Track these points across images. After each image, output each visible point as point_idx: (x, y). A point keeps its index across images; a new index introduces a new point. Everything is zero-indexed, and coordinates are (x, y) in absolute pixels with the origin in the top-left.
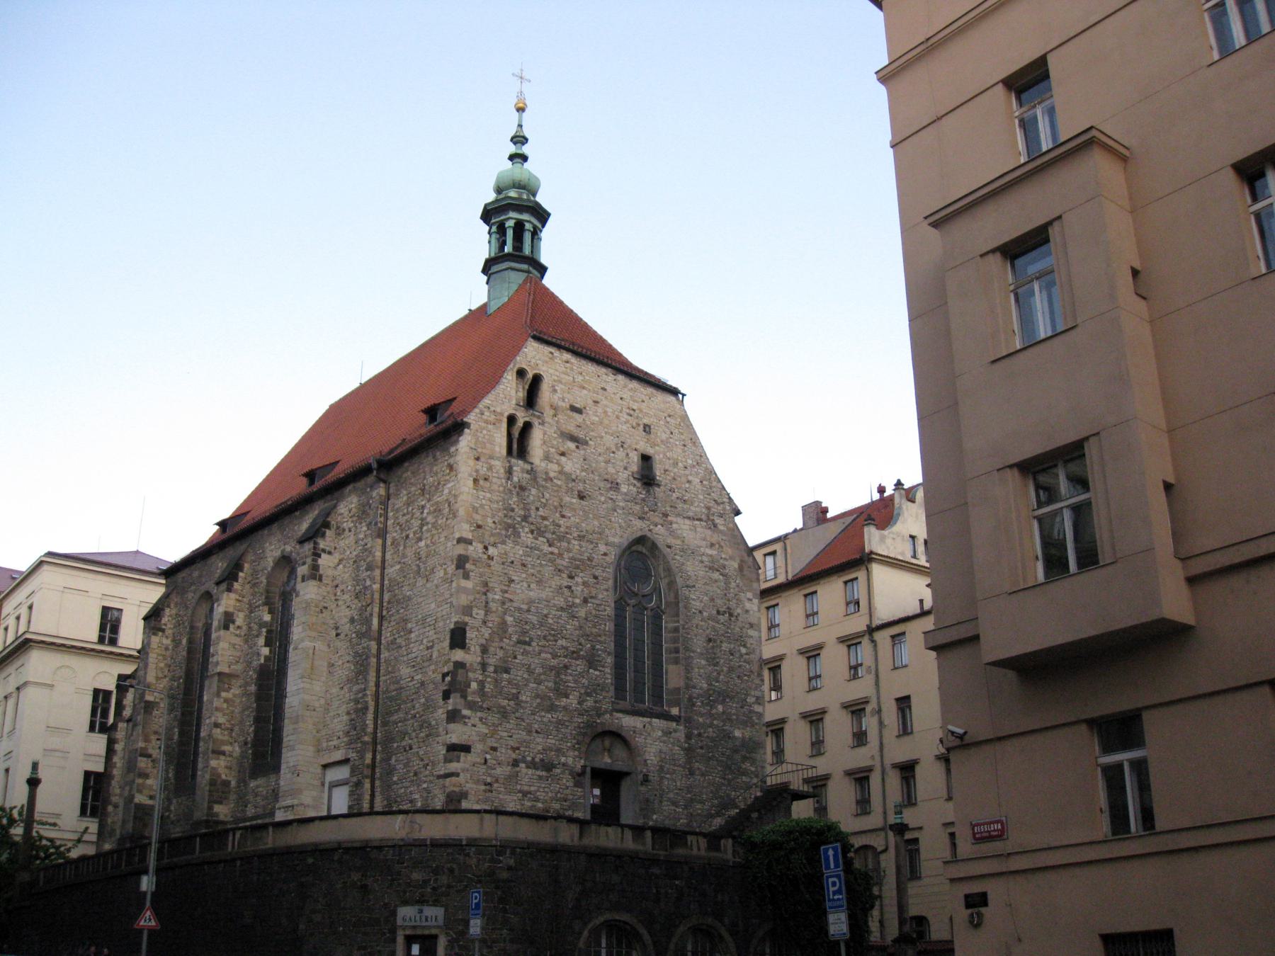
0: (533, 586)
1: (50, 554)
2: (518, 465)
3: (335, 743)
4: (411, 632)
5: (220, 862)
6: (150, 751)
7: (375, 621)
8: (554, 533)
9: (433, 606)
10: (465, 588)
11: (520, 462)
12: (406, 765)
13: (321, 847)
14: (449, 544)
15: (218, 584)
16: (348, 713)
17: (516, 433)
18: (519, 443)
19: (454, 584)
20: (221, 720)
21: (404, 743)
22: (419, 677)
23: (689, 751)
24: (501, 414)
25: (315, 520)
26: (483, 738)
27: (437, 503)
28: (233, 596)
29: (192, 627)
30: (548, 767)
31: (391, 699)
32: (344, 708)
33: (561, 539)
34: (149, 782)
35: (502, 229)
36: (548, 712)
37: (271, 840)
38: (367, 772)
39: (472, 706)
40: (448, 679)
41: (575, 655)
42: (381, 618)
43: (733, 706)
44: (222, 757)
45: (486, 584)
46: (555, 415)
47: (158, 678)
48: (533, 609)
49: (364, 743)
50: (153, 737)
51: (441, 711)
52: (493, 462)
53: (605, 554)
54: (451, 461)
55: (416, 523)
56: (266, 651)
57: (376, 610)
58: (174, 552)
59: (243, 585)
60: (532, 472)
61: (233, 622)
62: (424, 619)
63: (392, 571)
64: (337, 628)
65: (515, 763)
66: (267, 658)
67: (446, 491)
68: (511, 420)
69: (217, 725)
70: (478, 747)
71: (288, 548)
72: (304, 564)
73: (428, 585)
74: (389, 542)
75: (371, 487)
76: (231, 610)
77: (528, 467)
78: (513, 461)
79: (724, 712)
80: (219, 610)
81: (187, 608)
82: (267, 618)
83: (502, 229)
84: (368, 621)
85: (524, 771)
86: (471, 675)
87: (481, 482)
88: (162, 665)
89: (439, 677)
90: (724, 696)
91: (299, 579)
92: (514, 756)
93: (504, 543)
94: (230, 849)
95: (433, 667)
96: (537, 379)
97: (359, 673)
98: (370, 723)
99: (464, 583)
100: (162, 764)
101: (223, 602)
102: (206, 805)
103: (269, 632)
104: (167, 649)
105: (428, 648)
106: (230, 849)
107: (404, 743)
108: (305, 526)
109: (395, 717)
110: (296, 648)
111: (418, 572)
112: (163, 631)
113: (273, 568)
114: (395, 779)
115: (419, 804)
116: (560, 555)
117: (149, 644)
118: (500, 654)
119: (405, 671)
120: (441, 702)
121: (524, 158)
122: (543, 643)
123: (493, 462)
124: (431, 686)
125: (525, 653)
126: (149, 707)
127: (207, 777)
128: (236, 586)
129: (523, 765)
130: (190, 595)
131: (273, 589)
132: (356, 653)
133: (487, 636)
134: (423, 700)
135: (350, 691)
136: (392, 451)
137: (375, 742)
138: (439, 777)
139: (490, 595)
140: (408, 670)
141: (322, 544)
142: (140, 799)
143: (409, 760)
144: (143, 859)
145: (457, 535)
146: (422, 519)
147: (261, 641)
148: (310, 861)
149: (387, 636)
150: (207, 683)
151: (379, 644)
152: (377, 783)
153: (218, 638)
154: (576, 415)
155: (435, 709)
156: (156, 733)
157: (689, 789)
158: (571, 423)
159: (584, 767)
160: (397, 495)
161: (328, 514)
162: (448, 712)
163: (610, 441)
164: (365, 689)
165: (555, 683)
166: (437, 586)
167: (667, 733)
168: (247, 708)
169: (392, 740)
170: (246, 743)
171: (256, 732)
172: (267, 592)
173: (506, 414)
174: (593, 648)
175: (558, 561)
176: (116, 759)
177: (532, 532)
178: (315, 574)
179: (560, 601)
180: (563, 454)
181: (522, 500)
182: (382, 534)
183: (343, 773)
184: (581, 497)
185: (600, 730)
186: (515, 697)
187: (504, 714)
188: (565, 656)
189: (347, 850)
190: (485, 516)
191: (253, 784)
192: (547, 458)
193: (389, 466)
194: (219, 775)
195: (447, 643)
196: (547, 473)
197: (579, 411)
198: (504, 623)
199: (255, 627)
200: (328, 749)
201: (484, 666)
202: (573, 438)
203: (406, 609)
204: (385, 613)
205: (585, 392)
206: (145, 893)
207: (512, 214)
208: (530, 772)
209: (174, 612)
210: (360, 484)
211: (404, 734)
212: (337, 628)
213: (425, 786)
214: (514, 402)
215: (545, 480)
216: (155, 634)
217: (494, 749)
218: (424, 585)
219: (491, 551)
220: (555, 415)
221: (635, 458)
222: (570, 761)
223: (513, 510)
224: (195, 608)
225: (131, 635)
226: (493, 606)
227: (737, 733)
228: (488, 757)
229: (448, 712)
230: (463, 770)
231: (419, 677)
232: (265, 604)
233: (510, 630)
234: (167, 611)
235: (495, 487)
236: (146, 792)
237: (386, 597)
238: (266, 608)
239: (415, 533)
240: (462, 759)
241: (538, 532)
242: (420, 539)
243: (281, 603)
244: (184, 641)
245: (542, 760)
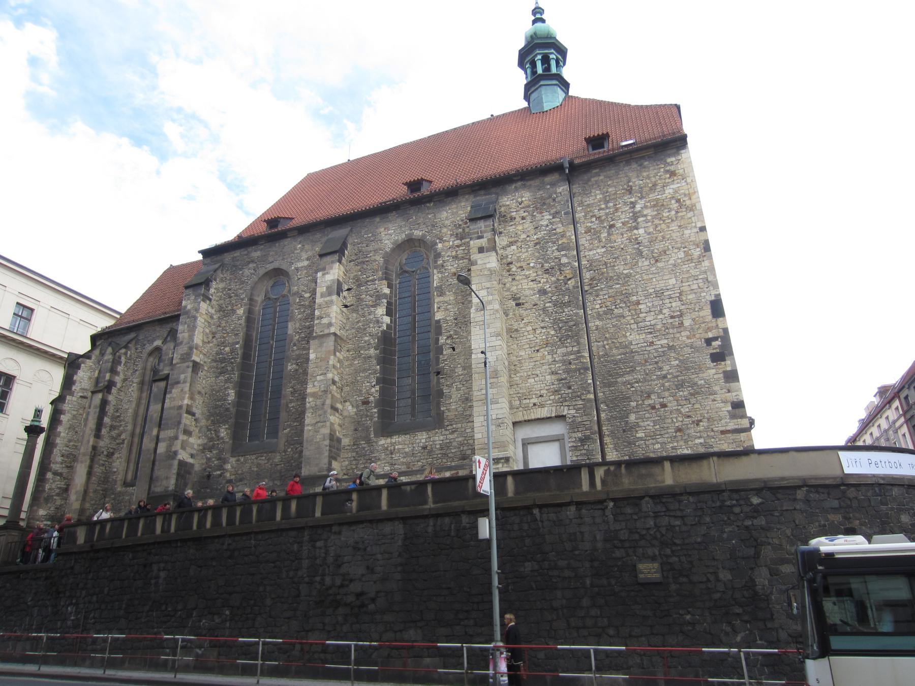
3: (535, 400)
4: (638, 303)
5: (568, 504)
6: (194, 410)
9: (673, 281)
14: (687, 232)
20: (337, 379)
21: (651, 402)
22: (666, 341)
29: (251, 300)
31: (616, 363)
34: (192, 440)
35: (546, 60)
37: (668, 477)
38: (596, 428)
40: (716, 344)
44: (337, 415)
47: (204, 342)
49: (589, 400)
50: (197, 396)
51: (713, 371)
54: (672, 168)
55: (624, 216)
56: (387, 320)
63: (593, 252)
64: (515, 299)
66: (388, 325)
67: (669, 191)
69: (334, 382)
71: (418, 233)
72: (482, 237)
73: (659, 264)
74: (581, 229)
75: (553, 185)
76: (341, 279)
81: (243, 282)
82: (387, 291)
83: (546, 60)
88: (207, 331)
89: (701, 343)
91: (476, 250)
94: (585, 487)
98: (590, 381)
100: (203, 422)
102: (326, 460)
104: (212, 317)
105: (672, 317)
106: (585, 487)
109: (628, 378)
111: (640, 253)
112: (210, 300)
113: (393, 250)
114: (640, 434)
119: (635, 338)
121: (543, 21)
126: (196, 366)
127: (326, 431)
128: (344, 260)
130: (247, 272)
131: (390, 267)
132: (555, 322)
135: (551, 353)
138: (723, 432)
142: (183, 456)
143: (662, 419)
145: (699, 225)
146: (634, 213)
147: (381, 311)
148: (756, 500)
149: (595, 305)
152: (607, 440)
153: (329, 304)
155: (700, 369)
156: (199, 393)
160: (586, 193)
162: (725, 372)
166: (674, 265)
168: (365, 370)
169: (629, 399)
170: (366, 402)
171: (382, 392)
172: (386, 268)
176: (60, 429)
178: (493, 248)
182: (574, 222)
183: (557, 429)
191: (383, 441)
193: (572, 172)
194: (335, 431)
195: (707, 312)
199: (369, 300)
200: (526, 408)
204: (586, 288)
206: (488, 541)
207: (552, 51)
209: (221, 286)
210: (536, 182)
213: (702, 441)
216: (203, 301)
218: (651, 265)
224: (256, 283)
229: (725, 372)
232: (386, 279)
234: (214, 283)
236: (189, 450)
237: (587, 275)
238: (385, 282)
239: (623, 224)
242: (637, 229)
244: (241, 311)
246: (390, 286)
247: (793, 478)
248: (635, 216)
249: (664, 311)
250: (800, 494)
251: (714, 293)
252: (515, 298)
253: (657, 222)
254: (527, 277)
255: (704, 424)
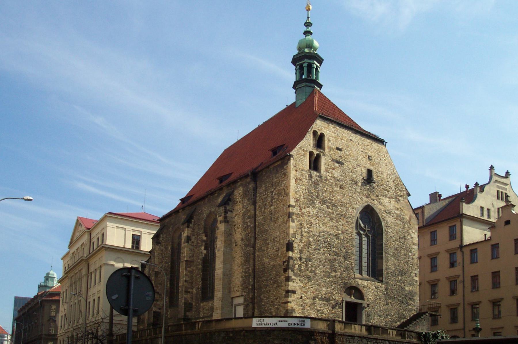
0: (321, 225)
1: (110, 213)
2: (315, 173)
4: (268, 244)
7: (253, 240)
8: (330, 203)
9: (278, 233)
10: (292, 226)
11: (315, 173)
12: (267, 298)
13: (237, 329)
15: (183, 224)
16: (242, 277)
17: (313, 159)
18: (315, 163)
19: (287, 224)
21: (266, 290)
22: (273, 263)
23: (386, 295)
24: (306, 151)
25: (224, 198)
26: (301, 288)
27: (279, 190)
28: (190, 229)
30: (328, 300)
32: (240, 275)
33: (333, 205)
36: (328, 278)
37: (214, 327)
39: (295, 275)
40: (286, 264)
41: (338, 255)
42: (255, 239)
43: (405, 278)
45: (301, 224)
46: (329, 152)
48: (321, 235)
51: (283, 276)
52: (303, 172)
53: (352, 212)
56: (205, 252)
57: (253, 235)
58: (162, 212)
59: (194, 225)
60: (320, 176)
61: (191, 240)
62: (274, 239)
65: (314, 298)
66: (205, 255)
68: (311, 153)
70: (299, 292)
73: (276, 225)
76: (189, 235)
77: (318, 174)
78: (312, 172)
79: (401, 280)
80: (185, 235)
82: (205, 238)
84: (249, 240)
85: (318, 301)
86: (295, 262)
87: (298, 181)
89: (281, 263)
90: (402, 273)
92: (314, 295)
93: (309, 207)
95: (278, 259)
96: (322, 136)
97: (246, 261)
99: (291, 224)
101: (186, 232)
103: (206, 244)
105: (276, 251)
107: (266, 290)
108: (220, 200)
110: (218, 251)
113: (206, 218)
115: (274, 314)
116: (333, 213)
117: (155, 249)
118: (308, 253)
119: (266, 260)
120: (283, 273)
122: (325, 249)
123: (303, 172)
124: (278, 267)
125: (318, 253)
128: (191, 225)
129: (317, 299)
130: (171, 229)
132: (245, 253)
133: (302, 246)
134: (274, 272)
135: (242, 268)
136: (259, 166)
137: (254, 289)
138: (282, 303)
139: (303, 229)
140: (268, 260)
141: (228, 208)
144: (161, 333)
147: (203, 248)
148: (231, 335)
149: (258, 246)
150: (181, 264)
151: (255, 249)
154: (339, 152)
157: (386, 311)
158: (337, 155)
159: (343, 300)
161: (230, 195)
162: (286, 277)
163: (354, 163)
164: (249, 268)
165: (331, 266)
166: (280, 225)
167: (377, 288)
173: (308, 151)
174: (346, 252)
175: (332, 215)
177: (320, 203)
179: (332, 232)
180: (333, 169)
181: (316, 188)
184: (341, 188)
185: (349, 285)
186: (314, 272)
187: (309, 279)
188: (335, 255)
189: (247, 331)
190: (300, 196)
192: (326, 170)
195: (285, 249)
196: (326, 177)
197: (340, 150)
198: (309, 241)
201: (301, 258)
202: (338, 162)
203: (266, 235)
204: (256, 236)
205: (343, 141)
208: (320, 302)
211: (267, 286)
212: (236, 243)
214: (312, 146)
215: (326, 180)
217: (306, 292)
218: (274, 225)
219: (303, 210)
220: (329, 152)
221: (365, 171)
222: (337, 298)
223: (312, 193)
225: (147, 245)
226: (304, 234)
227: (407, 288)
228: (303, 295)
229: (286, 277)
230: (293, 300)
231: (273, 263)
233: (312, 244)
235: (304, 183)
237: (257, 230)
240: (292, 296)
241: (323, 202)
243: (210, 231)
245: (325, 297)
246: (206, 236)
247: (240, 328)
248: (273, 198)
249: (275, 248)
250: (242, 334)
251: (288, 239)
252: (236, 243)
253: (278, 202)
254: (239, 232)
255: (278, 299)
